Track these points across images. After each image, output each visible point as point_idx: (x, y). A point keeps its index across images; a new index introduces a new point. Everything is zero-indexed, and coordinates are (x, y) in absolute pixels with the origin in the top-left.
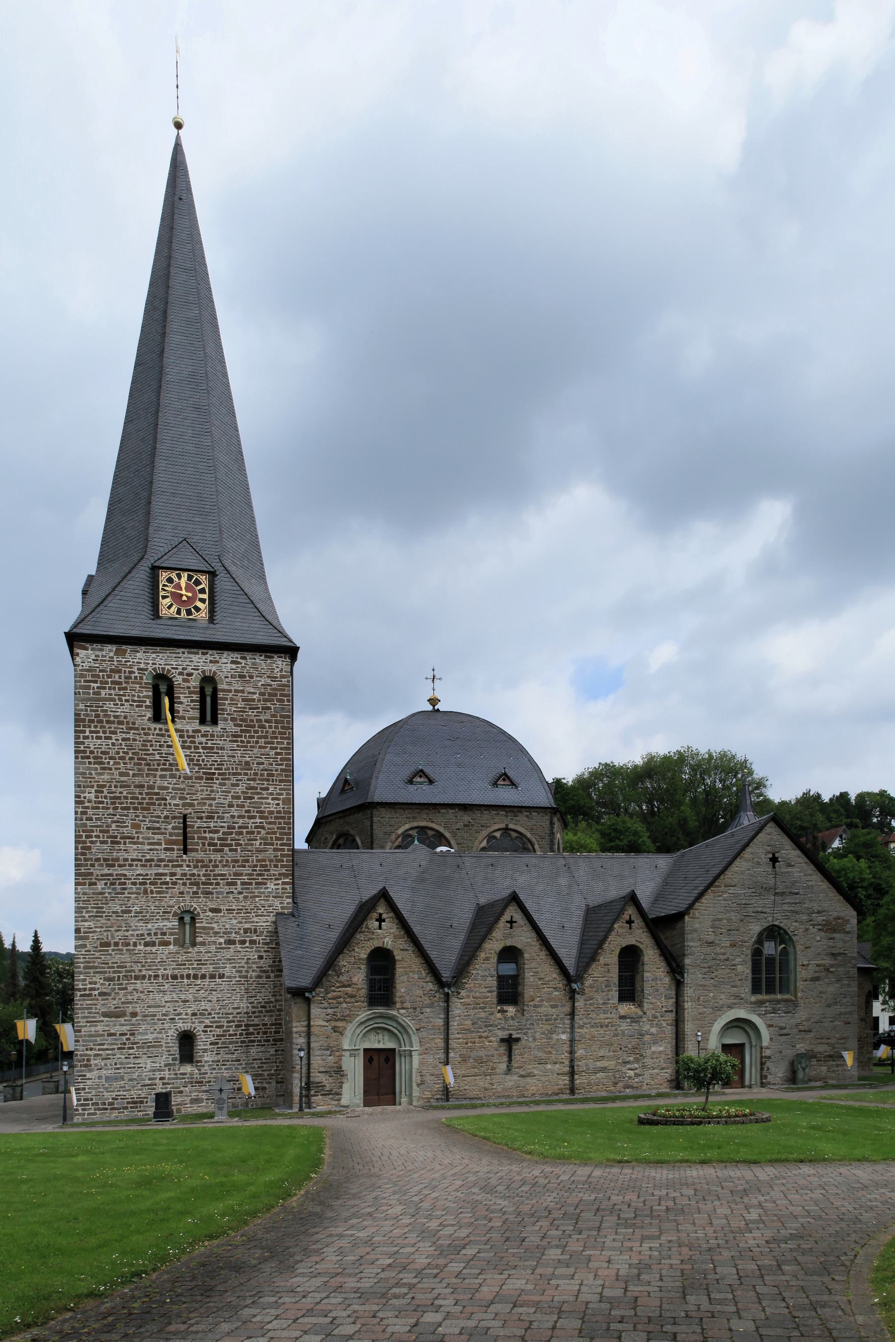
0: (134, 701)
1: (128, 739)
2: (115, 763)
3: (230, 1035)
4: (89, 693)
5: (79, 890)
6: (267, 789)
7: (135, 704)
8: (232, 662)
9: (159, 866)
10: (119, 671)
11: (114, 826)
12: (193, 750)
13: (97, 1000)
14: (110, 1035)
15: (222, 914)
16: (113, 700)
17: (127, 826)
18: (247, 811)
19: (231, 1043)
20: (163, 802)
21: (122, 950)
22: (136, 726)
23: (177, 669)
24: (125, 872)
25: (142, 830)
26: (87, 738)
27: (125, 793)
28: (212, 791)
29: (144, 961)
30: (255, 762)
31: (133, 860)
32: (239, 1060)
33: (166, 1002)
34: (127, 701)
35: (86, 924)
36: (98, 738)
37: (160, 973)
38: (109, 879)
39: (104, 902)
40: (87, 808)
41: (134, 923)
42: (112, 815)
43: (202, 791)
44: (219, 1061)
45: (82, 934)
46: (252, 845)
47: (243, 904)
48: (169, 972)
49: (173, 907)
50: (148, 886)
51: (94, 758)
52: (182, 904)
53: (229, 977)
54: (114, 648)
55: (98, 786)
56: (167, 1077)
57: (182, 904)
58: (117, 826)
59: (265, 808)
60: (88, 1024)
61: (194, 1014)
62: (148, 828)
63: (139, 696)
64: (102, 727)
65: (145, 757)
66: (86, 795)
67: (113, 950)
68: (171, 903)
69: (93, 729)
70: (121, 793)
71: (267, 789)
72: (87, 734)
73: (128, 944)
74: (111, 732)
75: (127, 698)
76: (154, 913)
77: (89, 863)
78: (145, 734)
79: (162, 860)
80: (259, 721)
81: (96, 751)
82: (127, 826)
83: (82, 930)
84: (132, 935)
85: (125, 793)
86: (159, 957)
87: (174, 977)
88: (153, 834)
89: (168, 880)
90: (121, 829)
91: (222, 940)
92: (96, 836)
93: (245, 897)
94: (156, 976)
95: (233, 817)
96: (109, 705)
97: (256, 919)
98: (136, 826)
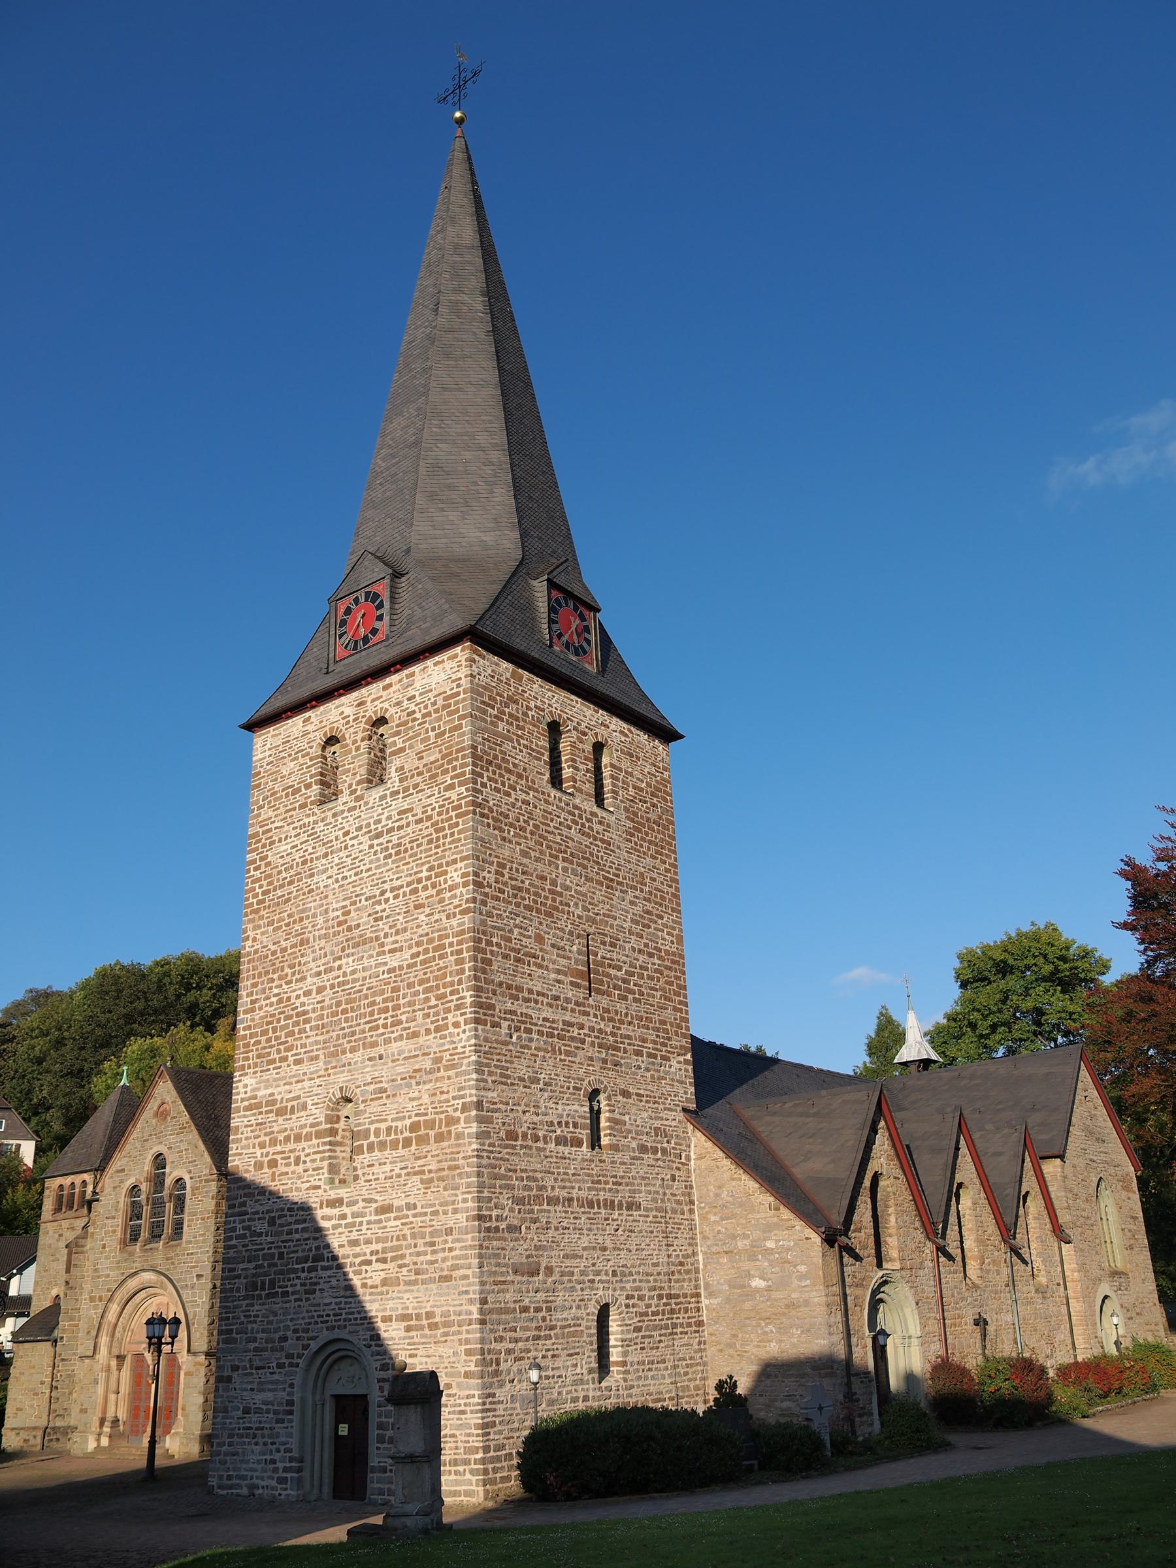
0: (532, 749)
1: (527, 803)
2: (516, 835)
3: (654, 1314)
4: (486, 721)
5: (480, 1032)
6: (661, 918)
7: (534, 754)
8: (621, 732)
9: (565, 1009)
10: (516, 702)
11: (516, 931)
12: (591, 840)
13: (505, 1239)
14: (525, 1309)
15: (631, 1101)
16: (512, 741)
17: (530, 937)
18: (646, 945)
19: (655, 1328)
20: (567, 908)
21: (531, 1148)
22: (536, 786)
23: (572, 721)
24: (530, 1012)
25: (545, 947)
26: (484, 785)
27: (527, 882)
28: (612, 906)
29: (555, 1171)
30: (649, 876)
31: (538, 994)
32: (664, 1361)
33: (584, 1249)
34: (525, 746)
35: (490, 1094)
36: (498, 790)
37: (575, 1196)
38: (513, 1020)
39: (508, 1058)
40: (486, 895)
41: (543, 1100)
42: (515, 914)
43: (603, 901)
44: (643, 1363)
45: (484, 1113)
46: (653, 996)
47: (649, 1087)
48: (583, 1194)
49: (583, 1080)
50: (556, 1040)
51: (495, 819)
52: (593, 1077)
53: (646, 1209)
54: (511, 666)
55: (500, 865)
56: (591, 1394)
57: (593, 1077)
58: (521, 934)
59: (662, 944)
60: (496, 1288)
61: (614, 1274)
62: (553, 946)
63: (537, 745)
64: (501, 775)
65: (547, 834)
66: (485, 874)
67: (522, 1147)
68: (581, 1072)
69: (490, 774)
70: (523, 882)
71: (661, 918)
72: (485, 780)
73: (536, 1139)
74: (510, 787)
75: (525, 742)
76: (562, 1087)
77: (491, 987)
78: (546, 802)
79: (568, 1000)
80: (648, 820)
81: (495, 808)
82: (530, 937)
83: (485, 1105)
84: (541, 1123)
85: (527, 882)
86: (572, 1167)
87: (591, 1205)
88: (558, 955)
89: (575, 1034)
90: (524, 940)
91: (634, 1145)
92: (498, 945)
93: (652, 1076)
94: (570, 1200)
95: (633, 949)
96: (507, 746)
97: (664, 1115)
98: (539, 939)
